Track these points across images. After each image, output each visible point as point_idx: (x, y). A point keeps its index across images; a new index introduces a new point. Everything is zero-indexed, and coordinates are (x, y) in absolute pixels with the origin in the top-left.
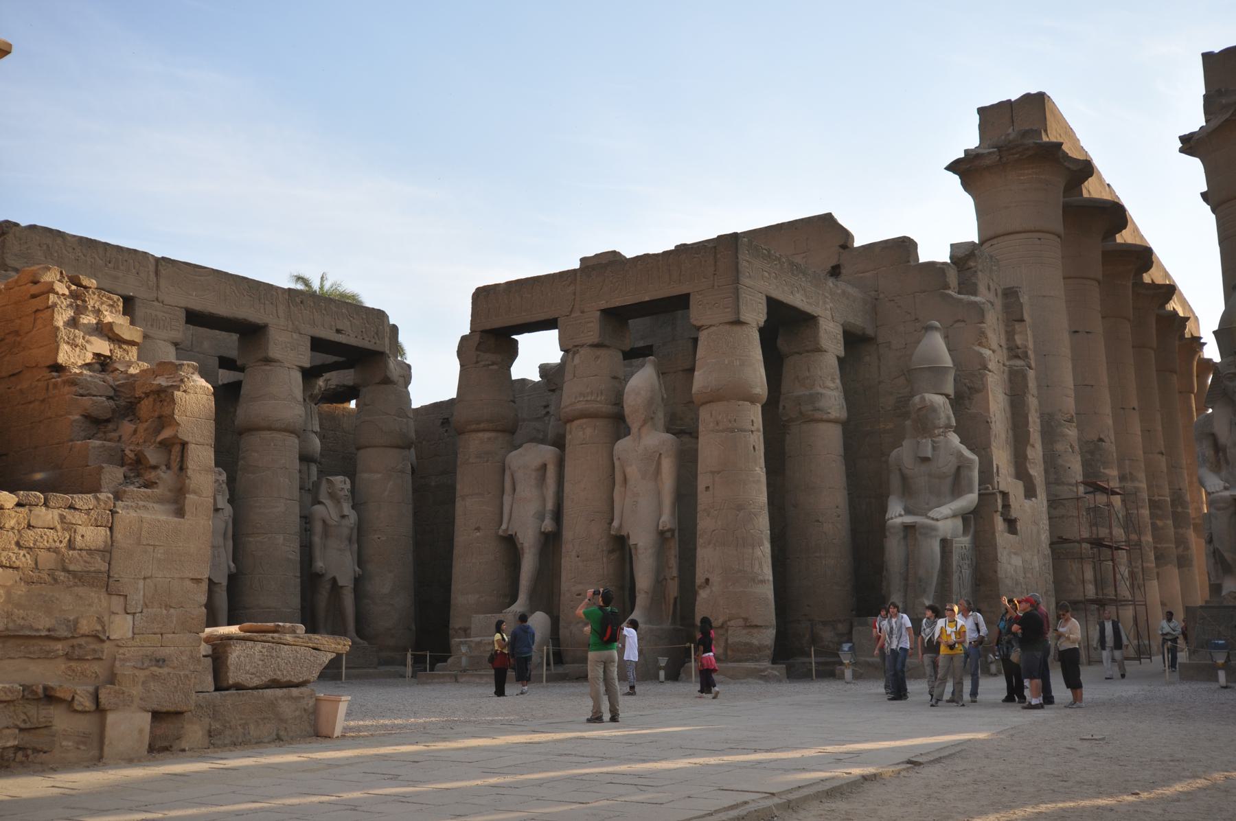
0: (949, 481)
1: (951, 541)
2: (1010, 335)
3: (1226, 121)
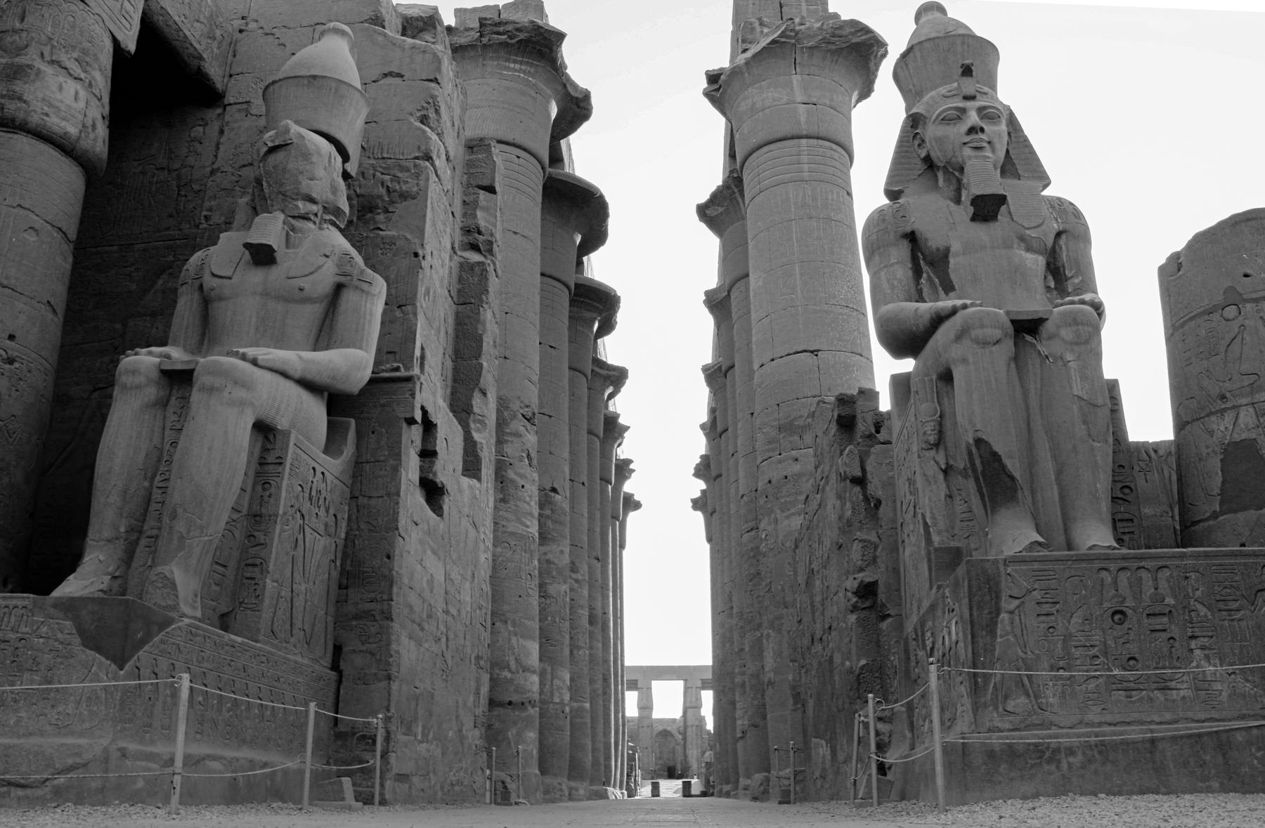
0: (311, 313)
1: (286, 434)
2: (469, 206)
3: (774, 42)
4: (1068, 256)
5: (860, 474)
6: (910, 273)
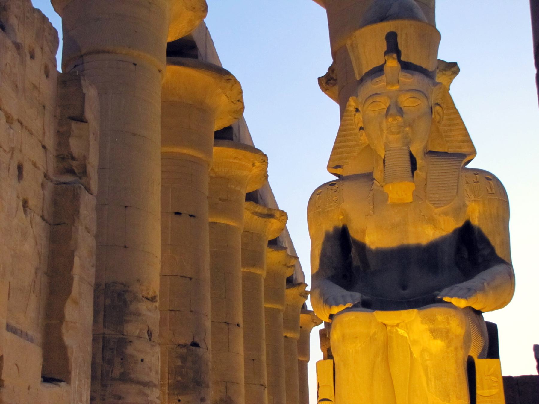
2: (63, 137)
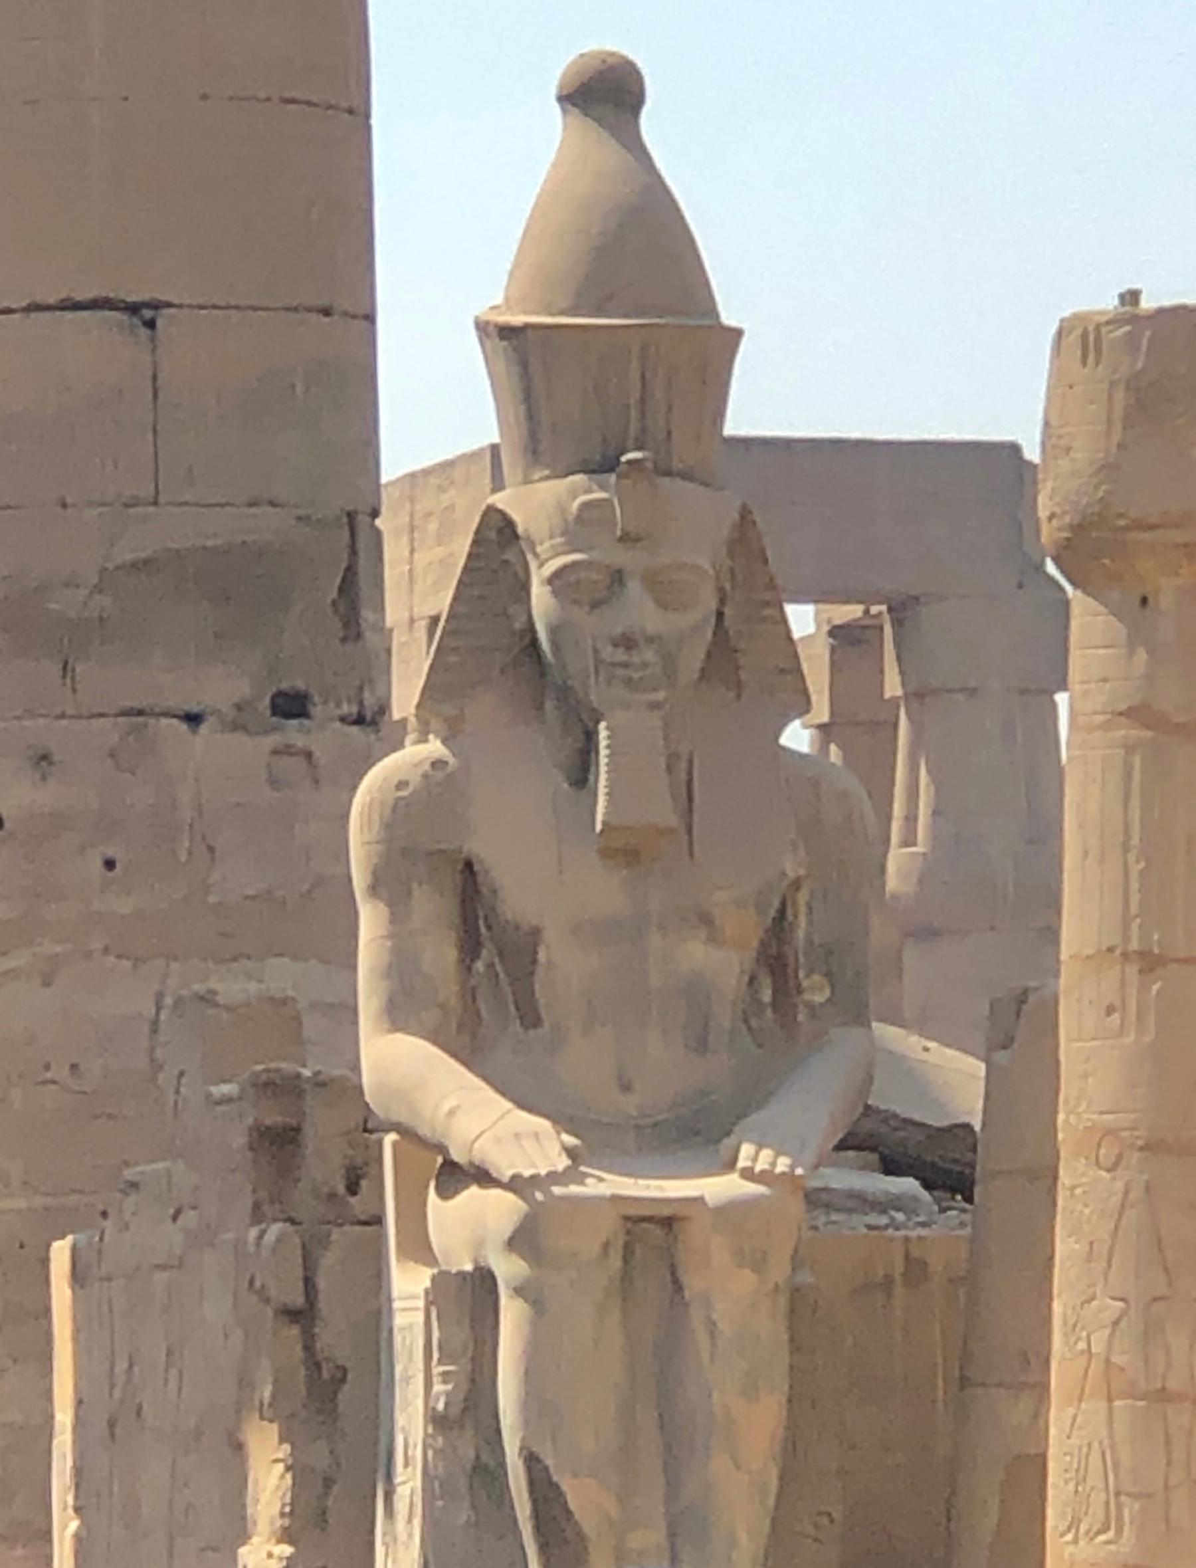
4: (808, 936)
5: (299, 1301)
6: (451, 955)
